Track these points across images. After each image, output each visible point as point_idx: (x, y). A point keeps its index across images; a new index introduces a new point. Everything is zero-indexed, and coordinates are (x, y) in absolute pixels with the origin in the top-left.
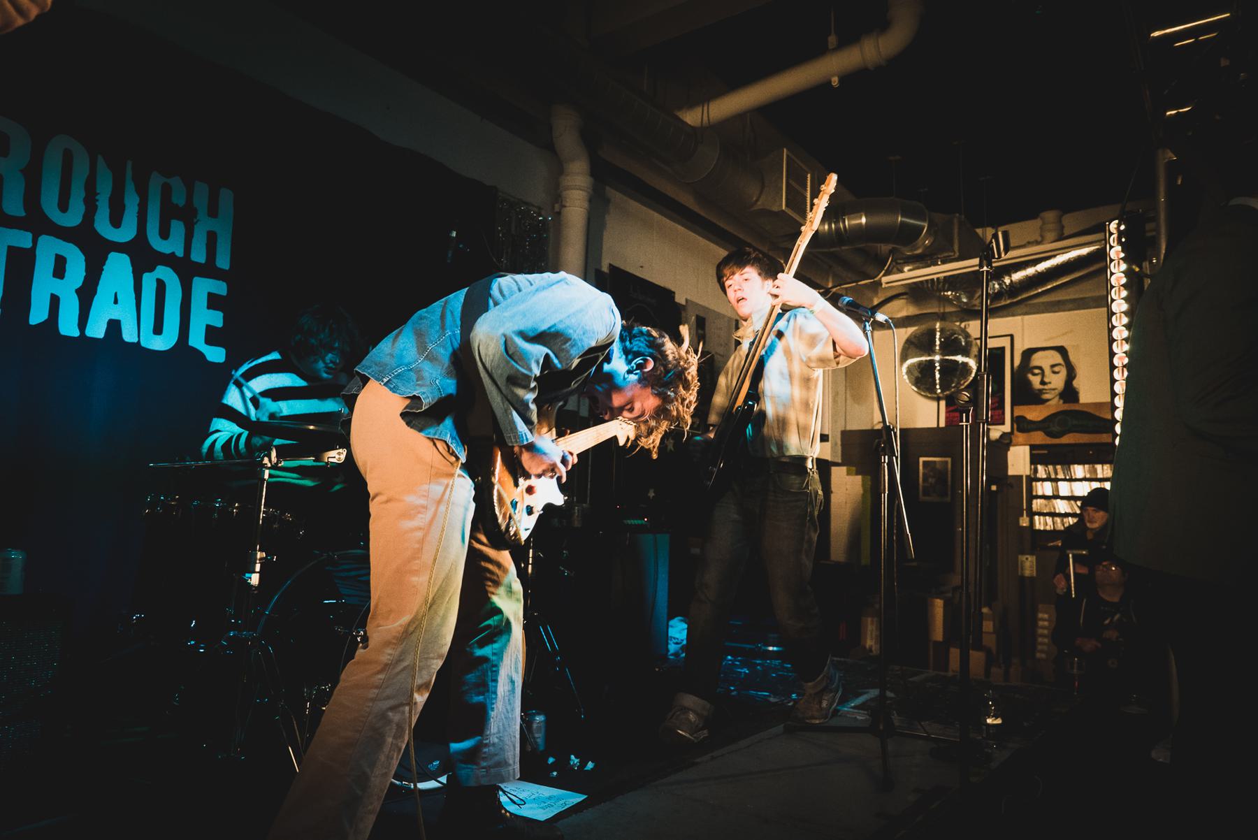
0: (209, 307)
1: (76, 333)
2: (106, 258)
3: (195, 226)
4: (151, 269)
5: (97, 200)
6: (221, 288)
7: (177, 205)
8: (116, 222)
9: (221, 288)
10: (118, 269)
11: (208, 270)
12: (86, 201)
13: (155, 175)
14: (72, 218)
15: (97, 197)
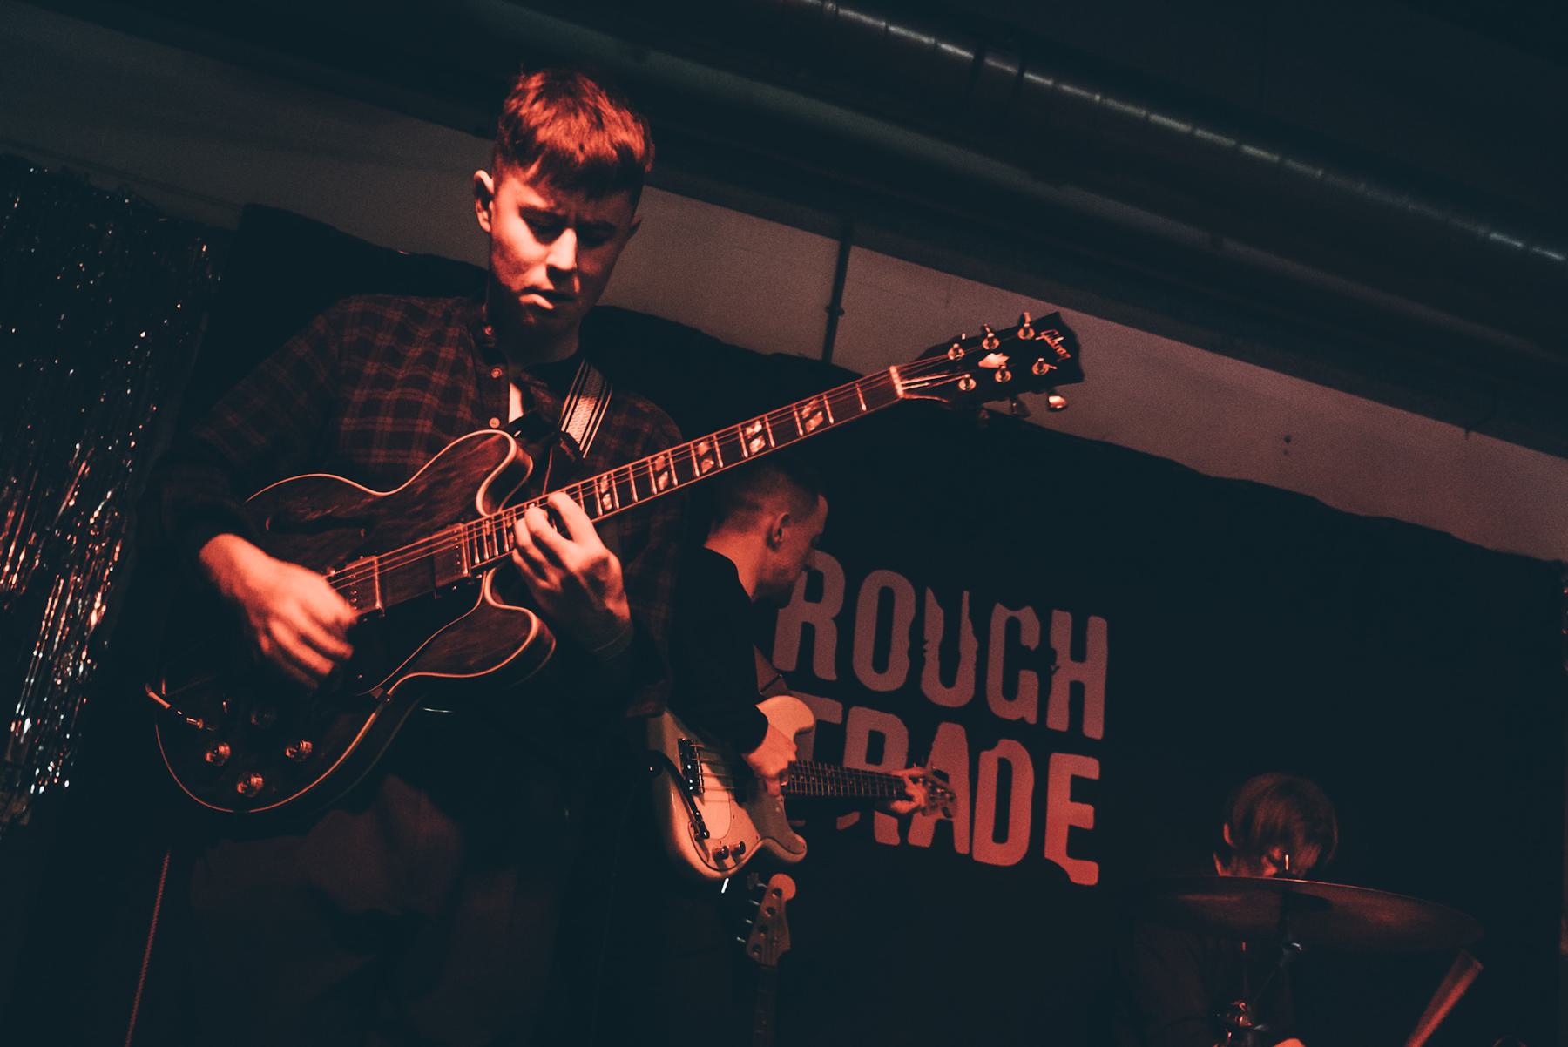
0: (1073, 799)
1: (895, 840)
2: (935, 732)
3: (1054, 677)
4: (991, 745)
5: (925, 651)
6: (1090, 768)
7: (1028, 647)
8: (948, 678)
9: (1090, 768)
10: (950, 744)
11: (1074, 742)
12: (910, 653)
13: (999, 607)
14: (892, 680)
15: (925, 647)
